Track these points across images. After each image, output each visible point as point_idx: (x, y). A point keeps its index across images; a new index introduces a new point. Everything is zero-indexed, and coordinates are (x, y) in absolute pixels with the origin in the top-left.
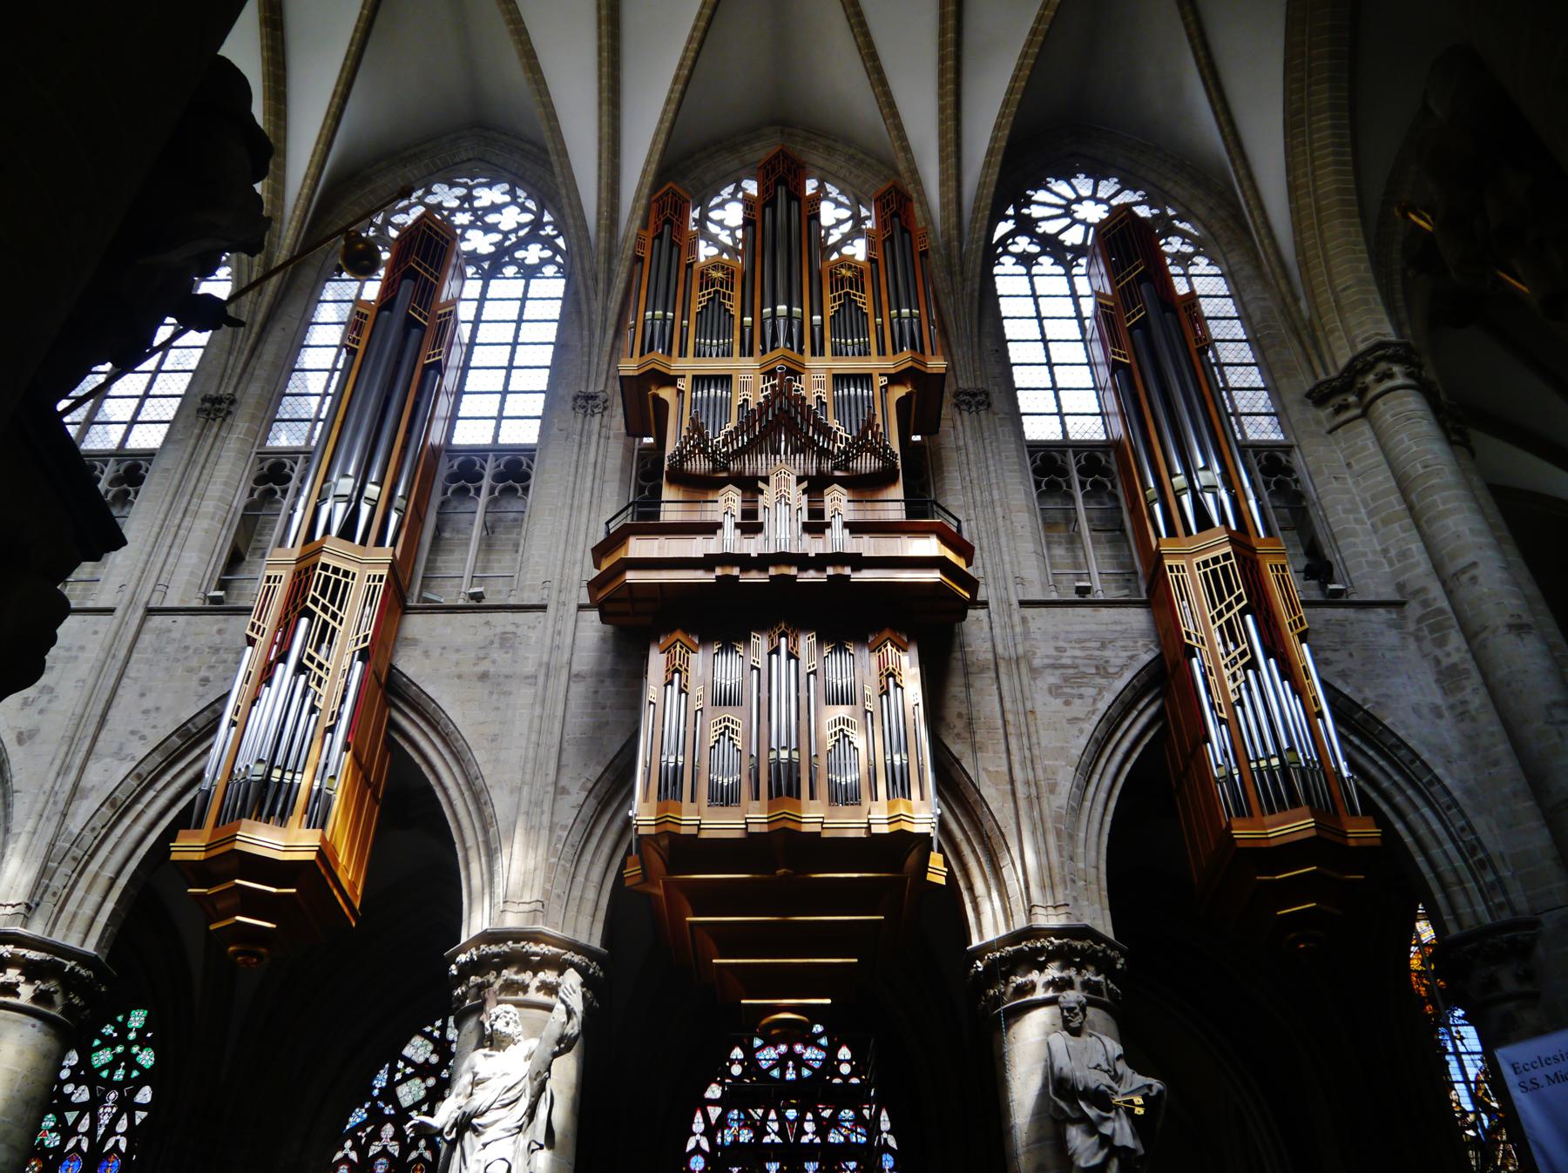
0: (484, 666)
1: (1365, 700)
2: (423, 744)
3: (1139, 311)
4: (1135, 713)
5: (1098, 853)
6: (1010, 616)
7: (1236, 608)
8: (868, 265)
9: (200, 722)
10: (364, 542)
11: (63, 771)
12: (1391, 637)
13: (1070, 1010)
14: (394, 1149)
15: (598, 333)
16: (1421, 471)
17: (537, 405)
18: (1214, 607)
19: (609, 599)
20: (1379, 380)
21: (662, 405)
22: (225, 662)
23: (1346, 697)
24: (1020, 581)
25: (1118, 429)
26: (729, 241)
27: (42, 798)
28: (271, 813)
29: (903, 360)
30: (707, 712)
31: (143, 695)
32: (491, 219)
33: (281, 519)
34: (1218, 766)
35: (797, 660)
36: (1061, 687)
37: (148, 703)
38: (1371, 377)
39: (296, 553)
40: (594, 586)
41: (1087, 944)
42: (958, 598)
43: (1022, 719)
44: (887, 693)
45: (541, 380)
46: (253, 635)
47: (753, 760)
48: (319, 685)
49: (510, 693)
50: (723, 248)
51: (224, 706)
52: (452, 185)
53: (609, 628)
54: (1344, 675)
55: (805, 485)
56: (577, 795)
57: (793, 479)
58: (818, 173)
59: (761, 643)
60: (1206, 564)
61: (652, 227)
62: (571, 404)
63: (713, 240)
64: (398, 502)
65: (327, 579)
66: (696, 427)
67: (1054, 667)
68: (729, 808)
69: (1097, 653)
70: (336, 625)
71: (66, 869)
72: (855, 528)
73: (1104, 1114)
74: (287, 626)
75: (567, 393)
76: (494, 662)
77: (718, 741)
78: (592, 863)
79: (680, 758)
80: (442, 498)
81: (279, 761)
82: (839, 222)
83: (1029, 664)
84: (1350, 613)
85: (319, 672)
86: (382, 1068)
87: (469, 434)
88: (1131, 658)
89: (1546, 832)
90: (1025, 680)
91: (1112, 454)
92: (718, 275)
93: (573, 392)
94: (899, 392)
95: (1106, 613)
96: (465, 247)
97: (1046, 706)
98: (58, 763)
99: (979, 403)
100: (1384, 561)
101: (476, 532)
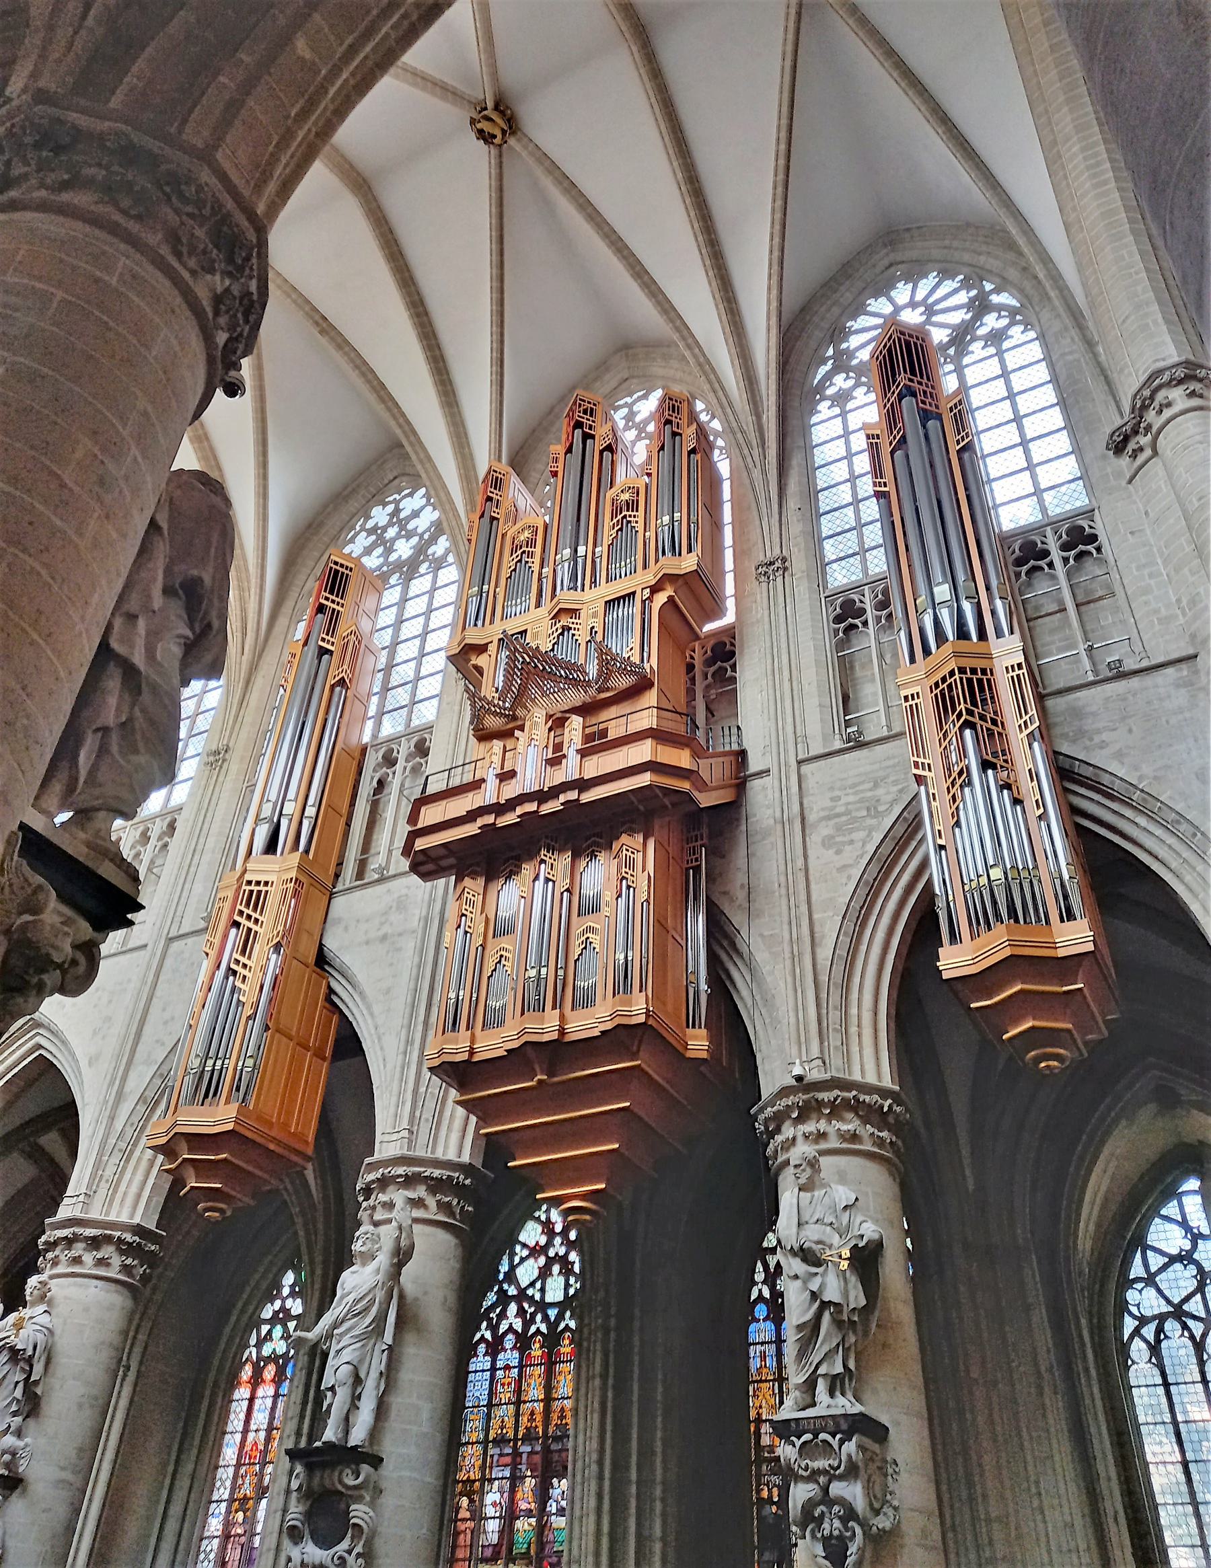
0: (386, 929)
11: (112, 1083)
12: (1180, 698)
14: (518, 1325)
31: (164, 1010)
32: (410, 526)
36: (833, 837)
52: (385, 504)
67: (828, 818)
69: (869, 794)
71: (115, 1160)
84: (1135, 682)
88: (901, 791)
95: (878, 749)
98: (109, 1077)
100: (1179, 612)
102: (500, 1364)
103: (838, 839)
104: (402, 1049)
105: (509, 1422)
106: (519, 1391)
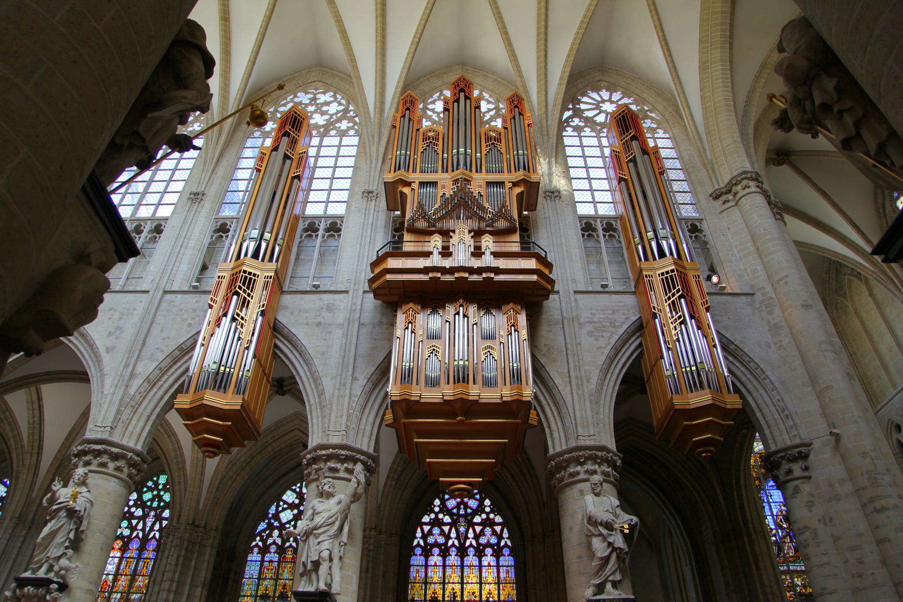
1: (735, 339)
2: (290, 355)
3: (632, 154)
4: (628, 345)
5: (610, 410)
6: (570, 298)
7: (677, 296)
8: (503, 130)
9: (188, 344)
10: (263, 260)
11: (127, 365)
13: (595, 484)
14: (279, 541)
15: (374, 161)
16: (762, 232)
17: (344, 196)
18: (666, 295)
19: (378, 288)
20: (744, 189)
21: (403, 196)
22: (199, 316)
23: (726, 338)
24: (574, 281)
25: (621, 210)
26: (436, 119)
27: (117, 378)
28: (220, 387)
29: (520, 175)
30: (425, 343)
31: (162, 331)
32: (325, 108)
33: (225, 249)
34: (667, 370)
35: (468, 318)
37: (165, 335)
38: (739, 187)
39: (232, 265)
40: (371, 281)
41: (604, 453)
42: (545, 289)
43: (575, 347)
44: (511, 334)
45: (346, 184)
46: (212, 303)
47: (446, 365)
48: (242, 327)
49: (330, 332)
50: (434, 122)
51: (198, 337)
52: (306, 93)
53: (379, 302)
54: (726, 328)
55: (472, 234)
56: (362, 381)
57: (466, 231)
58: (479, 87)
59: (450, 309)
60: (663, 274)
61: (400, 111)
62: (361, 195)
63: (429, 118)
64: (279, 241)
65: (246, 277)
66: (421, 206)
68: (435, 388)
69: (611, 316)
70: (250, 299)
71: (128, 411)
72: (496, 255)
73: (610, 533)
74: (228, 301)
75: (359, 190)
76: (323, 317)
77: (429, 356)
78: (369, 413)
79: (412, 364)
80: (300, 240)
81: (223, 362)
82: (489, 110)
83: (578, 320)
84: (729, 298)
85: (242, 321)
86: (273, 504)
87: (312, 210)
88: (627, 318)
89: (817, 402)
90: (576, 329)
91: (618, 222)
92: (431, 134)
93: (362, 190)
94: (518, 190)
95: (615, 296)
96: (312, 122)
97: (586, 341)
98: (124, 362)
99: (556, 197)
101: (316, 255)
102: (266, 559)
103: (596, 334)
104: (337, 387)
105: (271, 588)
106: (277, 573)
